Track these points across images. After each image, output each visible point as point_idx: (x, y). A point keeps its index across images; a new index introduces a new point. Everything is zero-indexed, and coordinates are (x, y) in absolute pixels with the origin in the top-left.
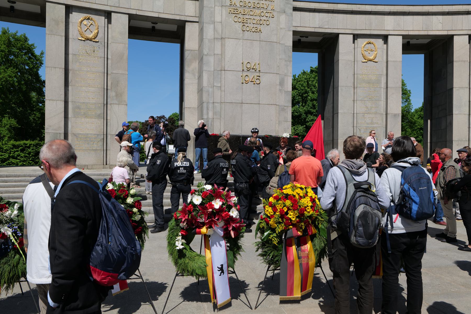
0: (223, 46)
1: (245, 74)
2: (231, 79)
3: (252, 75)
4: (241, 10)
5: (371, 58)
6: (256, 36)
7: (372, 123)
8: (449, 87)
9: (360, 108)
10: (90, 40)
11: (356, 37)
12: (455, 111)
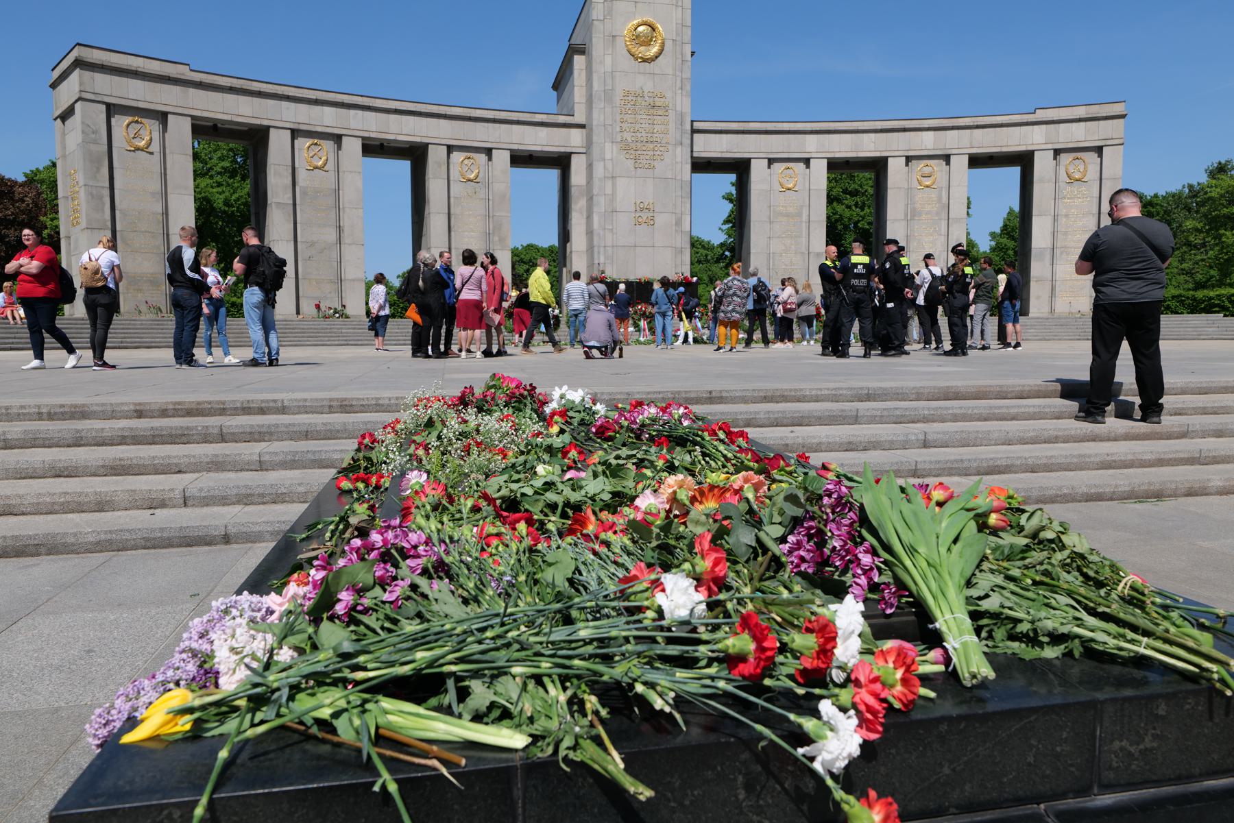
0: (614, 185)
3: (645, 216)
4: (633, 145)
11: (771, 161)
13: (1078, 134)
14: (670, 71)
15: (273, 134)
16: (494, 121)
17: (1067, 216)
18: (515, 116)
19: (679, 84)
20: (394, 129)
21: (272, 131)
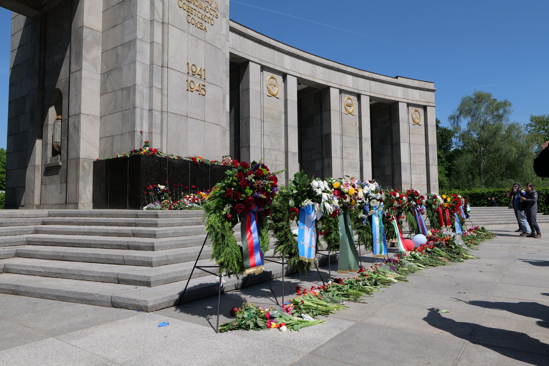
1: (190, 79)
2: (176, 81)
3: (198, 82)
5: (275, 93)
8: (325, 132)
12: (333, 155)
13: (416, 96)
17: (414, 144)
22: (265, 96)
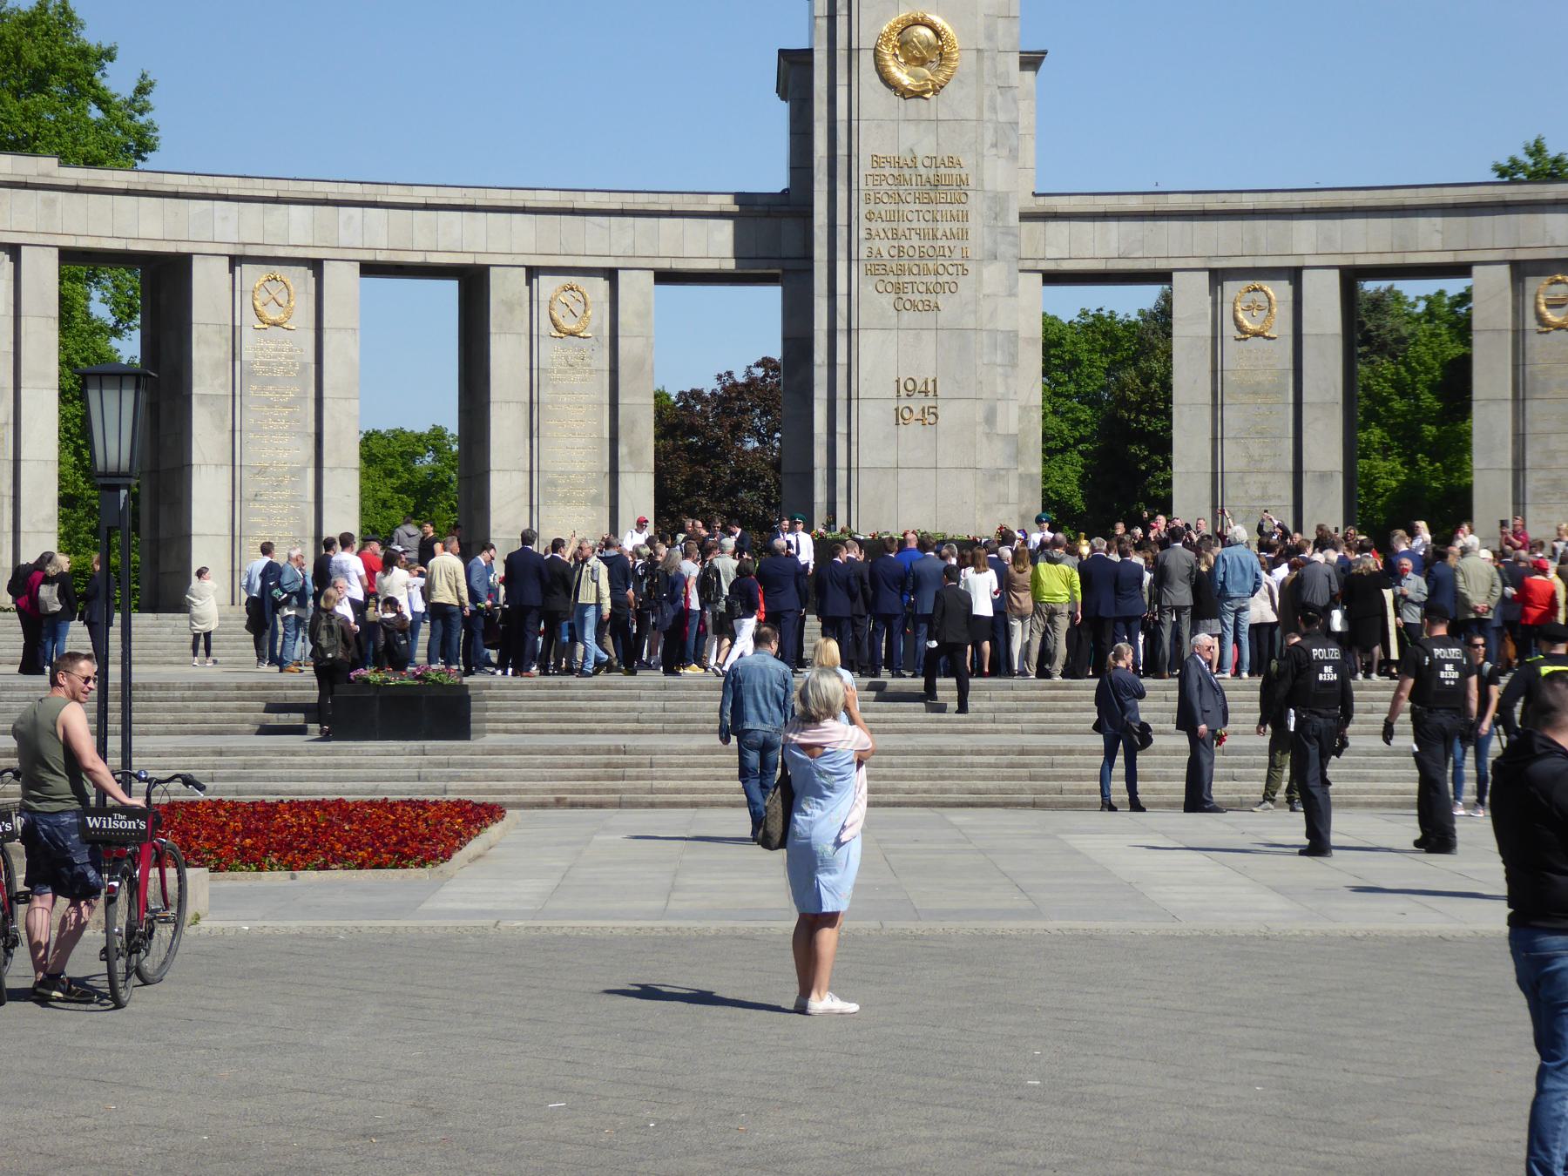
6: (927, 319)
7: (1262, 498)
9: (1233, 458)
10: (572, 334)
14: (971, 113)
15: (198, 266)
16: (622, 213)
18: (664, 203)
19: (989, 137)
20: (422, 242)
21: (196, 260)
22: (1229, 344)
